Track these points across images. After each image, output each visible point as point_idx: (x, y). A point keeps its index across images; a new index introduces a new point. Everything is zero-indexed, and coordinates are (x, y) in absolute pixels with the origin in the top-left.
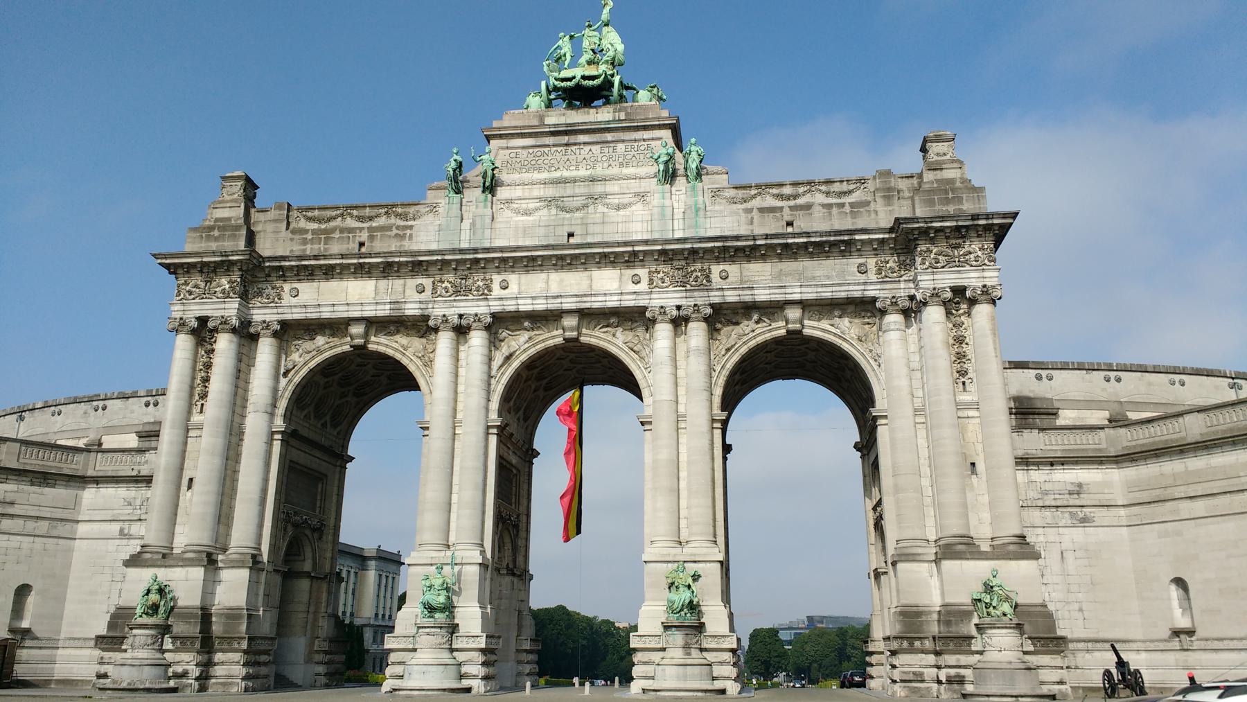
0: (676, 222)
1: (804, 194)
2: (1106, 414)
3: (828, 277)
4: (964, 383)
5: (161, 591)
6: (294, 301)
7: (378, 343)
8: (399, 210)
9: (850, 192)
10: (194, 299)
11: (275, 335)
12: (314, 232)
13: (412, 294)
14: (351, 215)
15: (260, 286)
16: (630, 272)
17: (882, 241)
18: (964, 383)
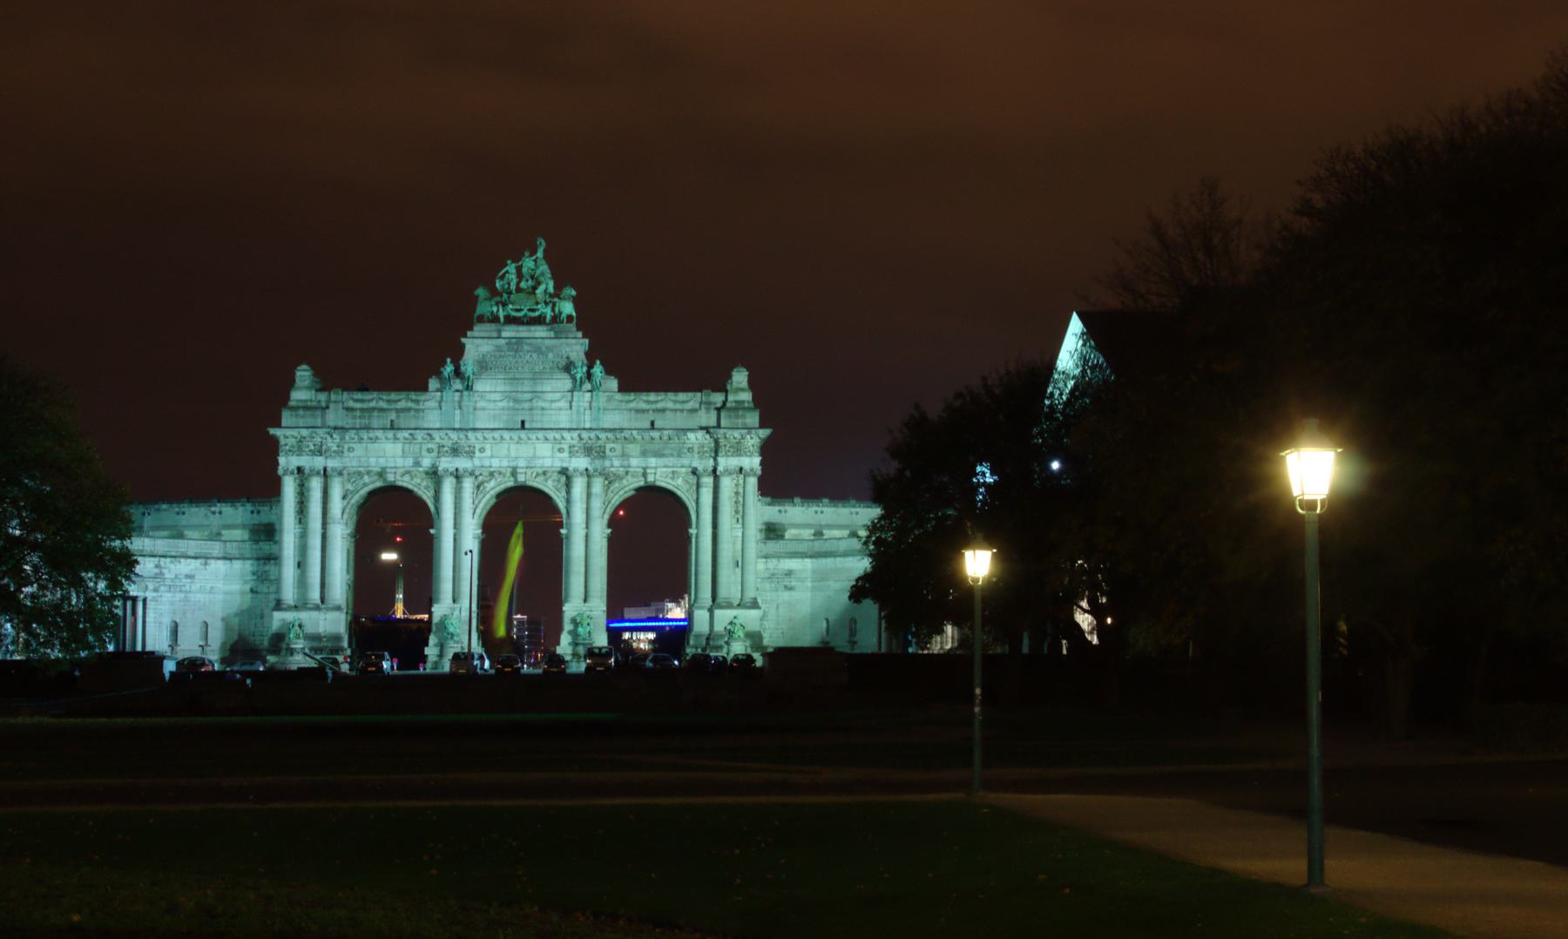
0: (586, 417)
1: (662, 400)
2: (813, 531)
3: (672, 455)
5: (300, 626)
6: (351, 455)
7: (403, 481)
12: (362, 410)
13: (424, 453)
16: (557, 446)
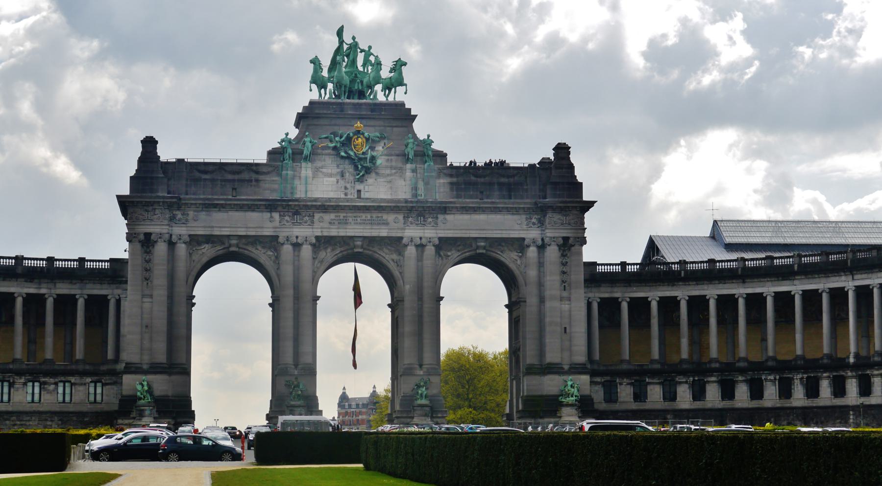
4: (565, 286)
6: (195, 224)
8: (254, 168)
9: (514, 176)
10: (141, 222)
11: (185, 243)
14: (226, 171)
15: (174, 213)
17: (529, 208)
18: (565, 286)
